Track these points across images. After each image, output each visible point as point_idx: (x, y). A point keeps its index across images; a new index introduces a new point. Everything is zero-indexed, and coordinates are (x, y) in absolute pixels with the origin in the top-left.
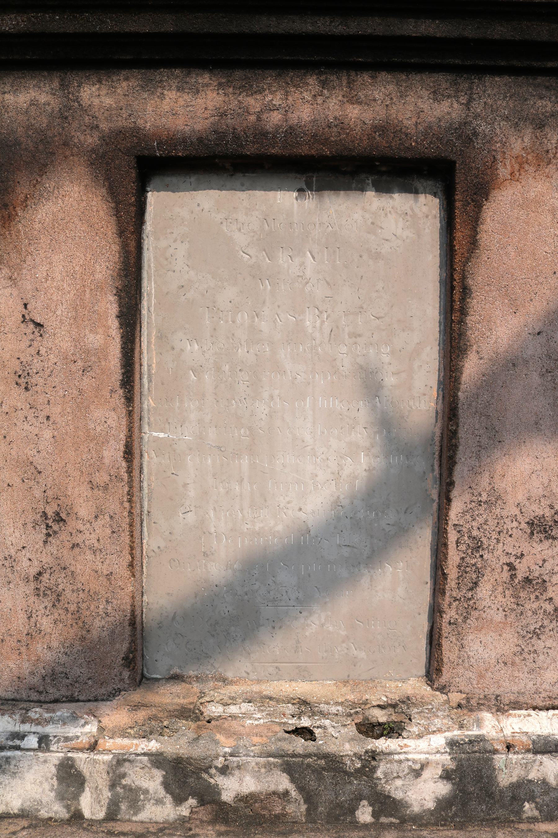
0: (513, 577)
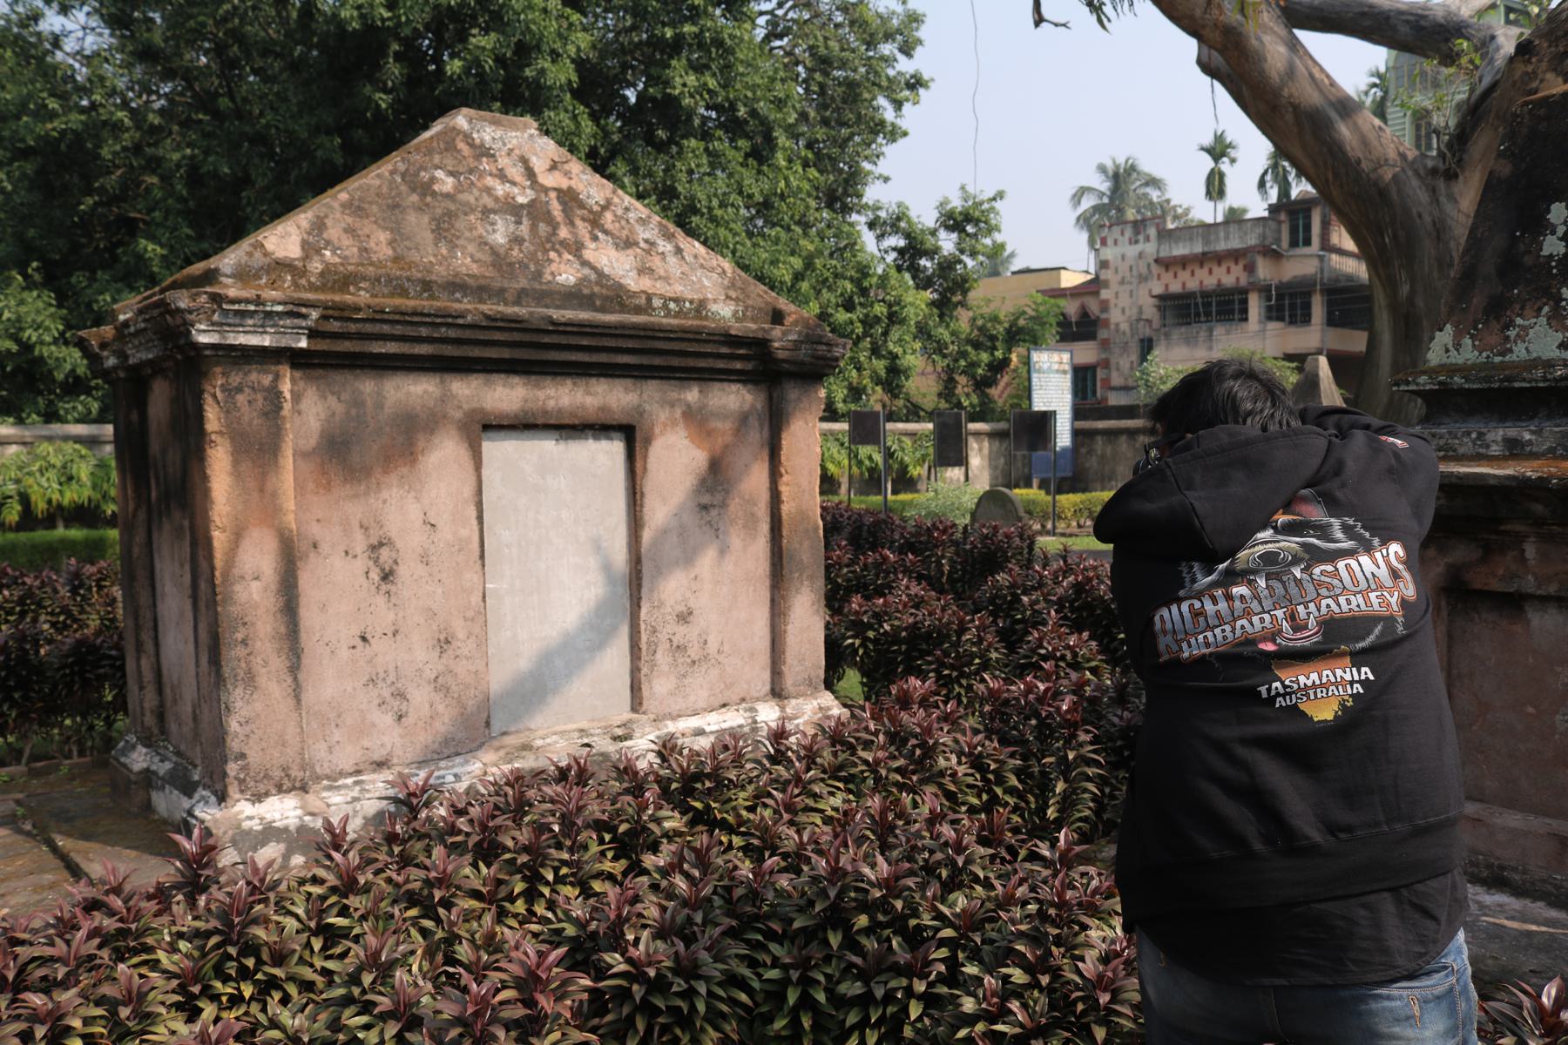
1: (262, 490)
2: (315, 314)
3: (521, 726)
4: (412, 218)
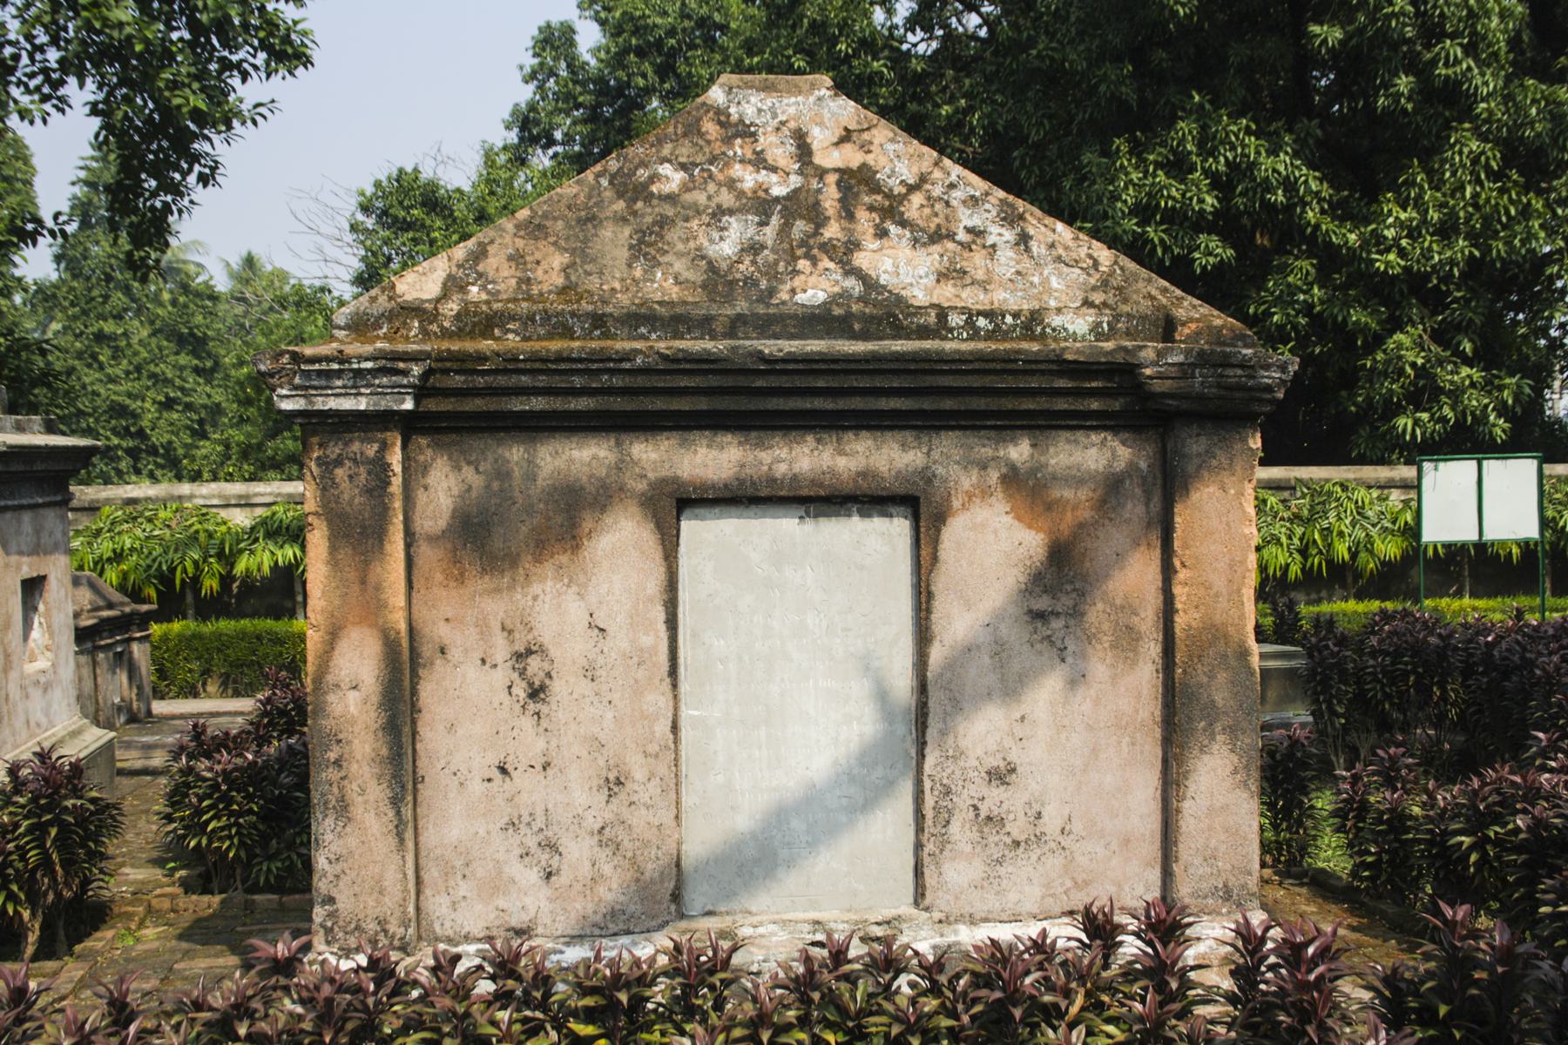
0: (977, 816)
1: (363, 582)
2: (416, 370)
3: (734, 906)
4: (607, 232)
